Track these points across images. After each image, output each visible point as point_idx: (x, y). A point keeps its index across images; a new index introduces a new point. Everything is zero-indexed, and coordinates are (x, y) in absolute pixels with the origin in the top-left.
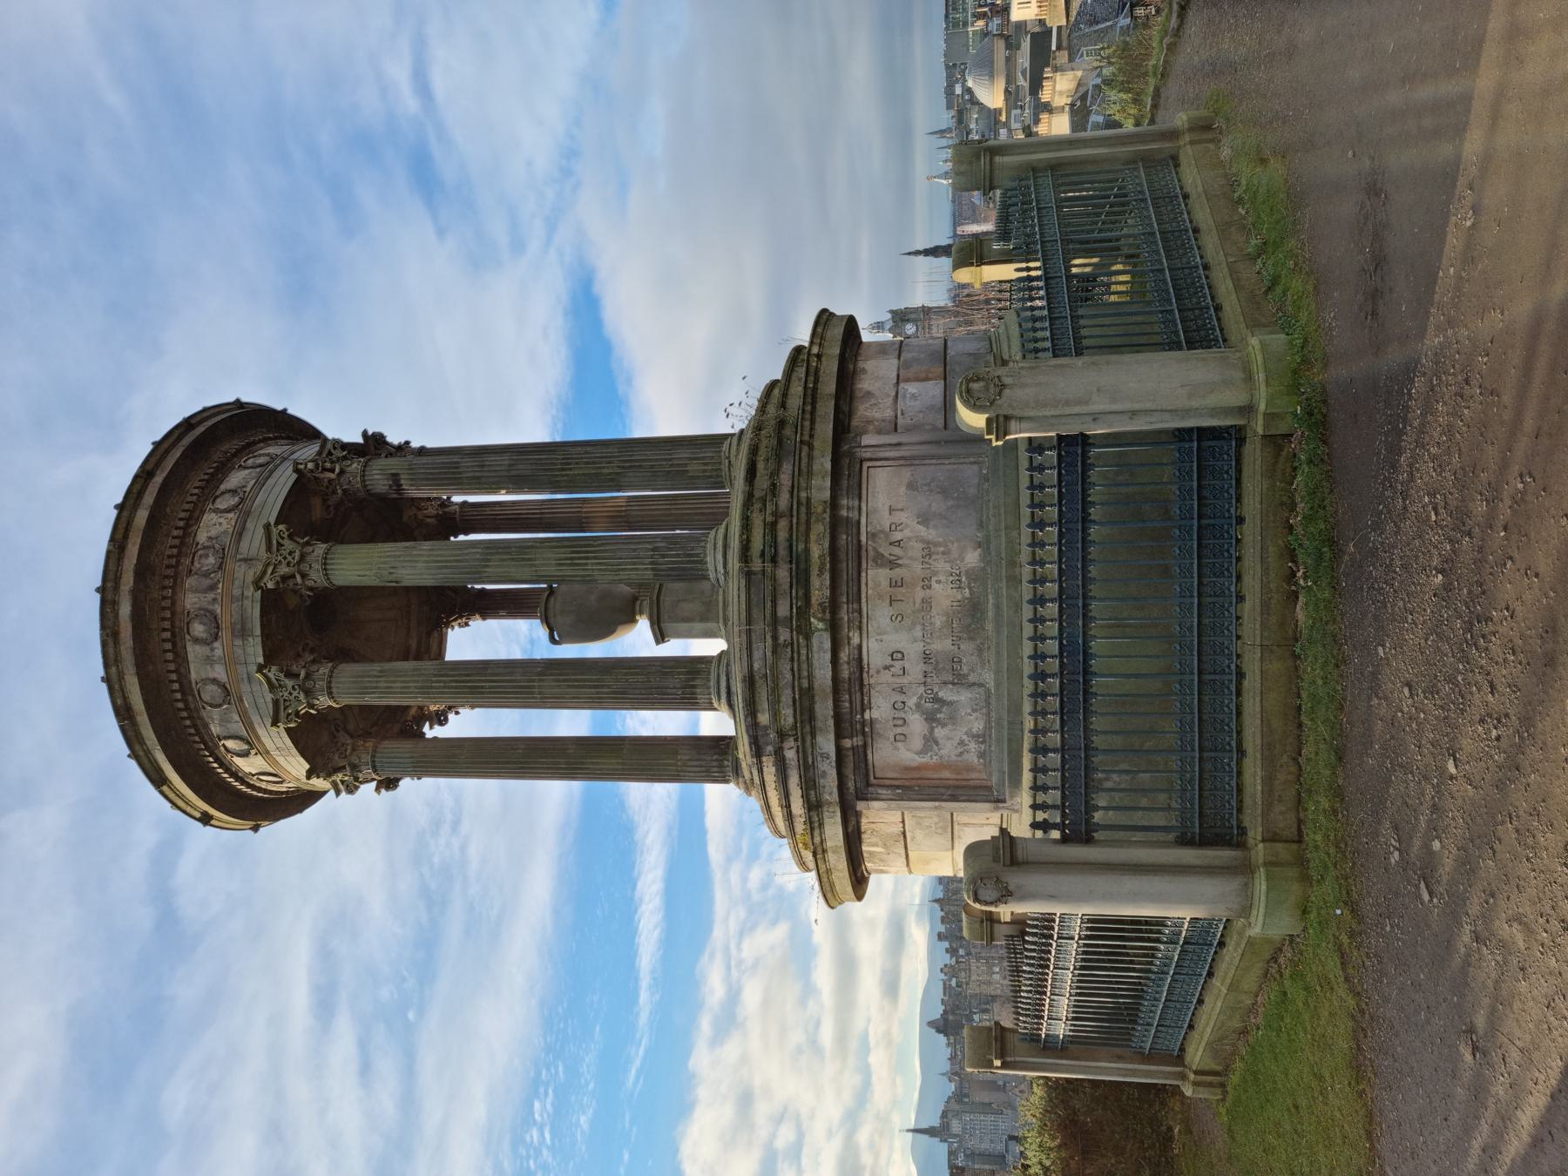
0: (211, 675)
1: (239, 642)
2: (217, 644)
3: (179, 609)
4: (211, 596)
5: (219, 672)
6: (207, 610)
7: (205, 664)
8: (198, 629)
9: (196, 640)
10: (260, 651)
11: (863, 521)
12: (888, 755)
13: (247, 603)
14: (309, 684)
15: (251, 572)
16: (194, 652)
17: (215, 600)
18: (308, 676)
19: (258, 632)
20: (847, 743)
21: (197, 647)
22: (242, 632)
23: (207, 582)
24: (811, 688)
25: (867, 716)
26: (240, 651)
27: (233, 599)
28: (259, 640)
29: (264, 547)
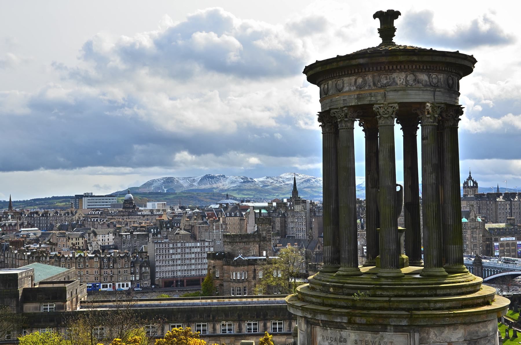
0: (345, 85)
1: (356, 97)
2: (355, 88)
3: (366, 73)
4: (372, 84)
5: (346, 89)
6: (366, 83)
7: (348, 83)
8: (360, 80)
9: (356, 80)
10: (353, 104)
11: (386, 333)
12: (318, 330)
13: (369, 98)
14: (343, 122)
15: (379, 98)
16: (353, 79)
17: (370, 86)
18: (346, 121)
19: (359, 104)
20: (320, 322)
21: (354, 80)
22: (359, 98)
23: (376, 82)
24: (332, 314)
25: (328, 328)
26: (353, 97)
27: (370, 94)
28: (356, 104)
29: (389, 101)
